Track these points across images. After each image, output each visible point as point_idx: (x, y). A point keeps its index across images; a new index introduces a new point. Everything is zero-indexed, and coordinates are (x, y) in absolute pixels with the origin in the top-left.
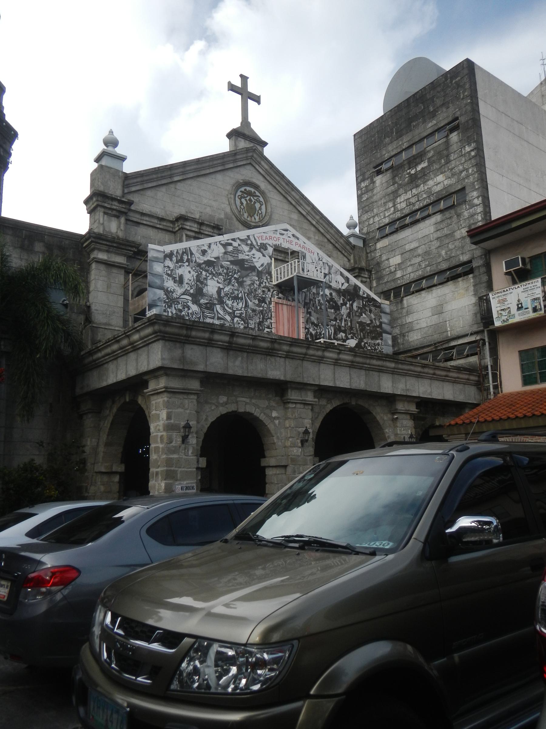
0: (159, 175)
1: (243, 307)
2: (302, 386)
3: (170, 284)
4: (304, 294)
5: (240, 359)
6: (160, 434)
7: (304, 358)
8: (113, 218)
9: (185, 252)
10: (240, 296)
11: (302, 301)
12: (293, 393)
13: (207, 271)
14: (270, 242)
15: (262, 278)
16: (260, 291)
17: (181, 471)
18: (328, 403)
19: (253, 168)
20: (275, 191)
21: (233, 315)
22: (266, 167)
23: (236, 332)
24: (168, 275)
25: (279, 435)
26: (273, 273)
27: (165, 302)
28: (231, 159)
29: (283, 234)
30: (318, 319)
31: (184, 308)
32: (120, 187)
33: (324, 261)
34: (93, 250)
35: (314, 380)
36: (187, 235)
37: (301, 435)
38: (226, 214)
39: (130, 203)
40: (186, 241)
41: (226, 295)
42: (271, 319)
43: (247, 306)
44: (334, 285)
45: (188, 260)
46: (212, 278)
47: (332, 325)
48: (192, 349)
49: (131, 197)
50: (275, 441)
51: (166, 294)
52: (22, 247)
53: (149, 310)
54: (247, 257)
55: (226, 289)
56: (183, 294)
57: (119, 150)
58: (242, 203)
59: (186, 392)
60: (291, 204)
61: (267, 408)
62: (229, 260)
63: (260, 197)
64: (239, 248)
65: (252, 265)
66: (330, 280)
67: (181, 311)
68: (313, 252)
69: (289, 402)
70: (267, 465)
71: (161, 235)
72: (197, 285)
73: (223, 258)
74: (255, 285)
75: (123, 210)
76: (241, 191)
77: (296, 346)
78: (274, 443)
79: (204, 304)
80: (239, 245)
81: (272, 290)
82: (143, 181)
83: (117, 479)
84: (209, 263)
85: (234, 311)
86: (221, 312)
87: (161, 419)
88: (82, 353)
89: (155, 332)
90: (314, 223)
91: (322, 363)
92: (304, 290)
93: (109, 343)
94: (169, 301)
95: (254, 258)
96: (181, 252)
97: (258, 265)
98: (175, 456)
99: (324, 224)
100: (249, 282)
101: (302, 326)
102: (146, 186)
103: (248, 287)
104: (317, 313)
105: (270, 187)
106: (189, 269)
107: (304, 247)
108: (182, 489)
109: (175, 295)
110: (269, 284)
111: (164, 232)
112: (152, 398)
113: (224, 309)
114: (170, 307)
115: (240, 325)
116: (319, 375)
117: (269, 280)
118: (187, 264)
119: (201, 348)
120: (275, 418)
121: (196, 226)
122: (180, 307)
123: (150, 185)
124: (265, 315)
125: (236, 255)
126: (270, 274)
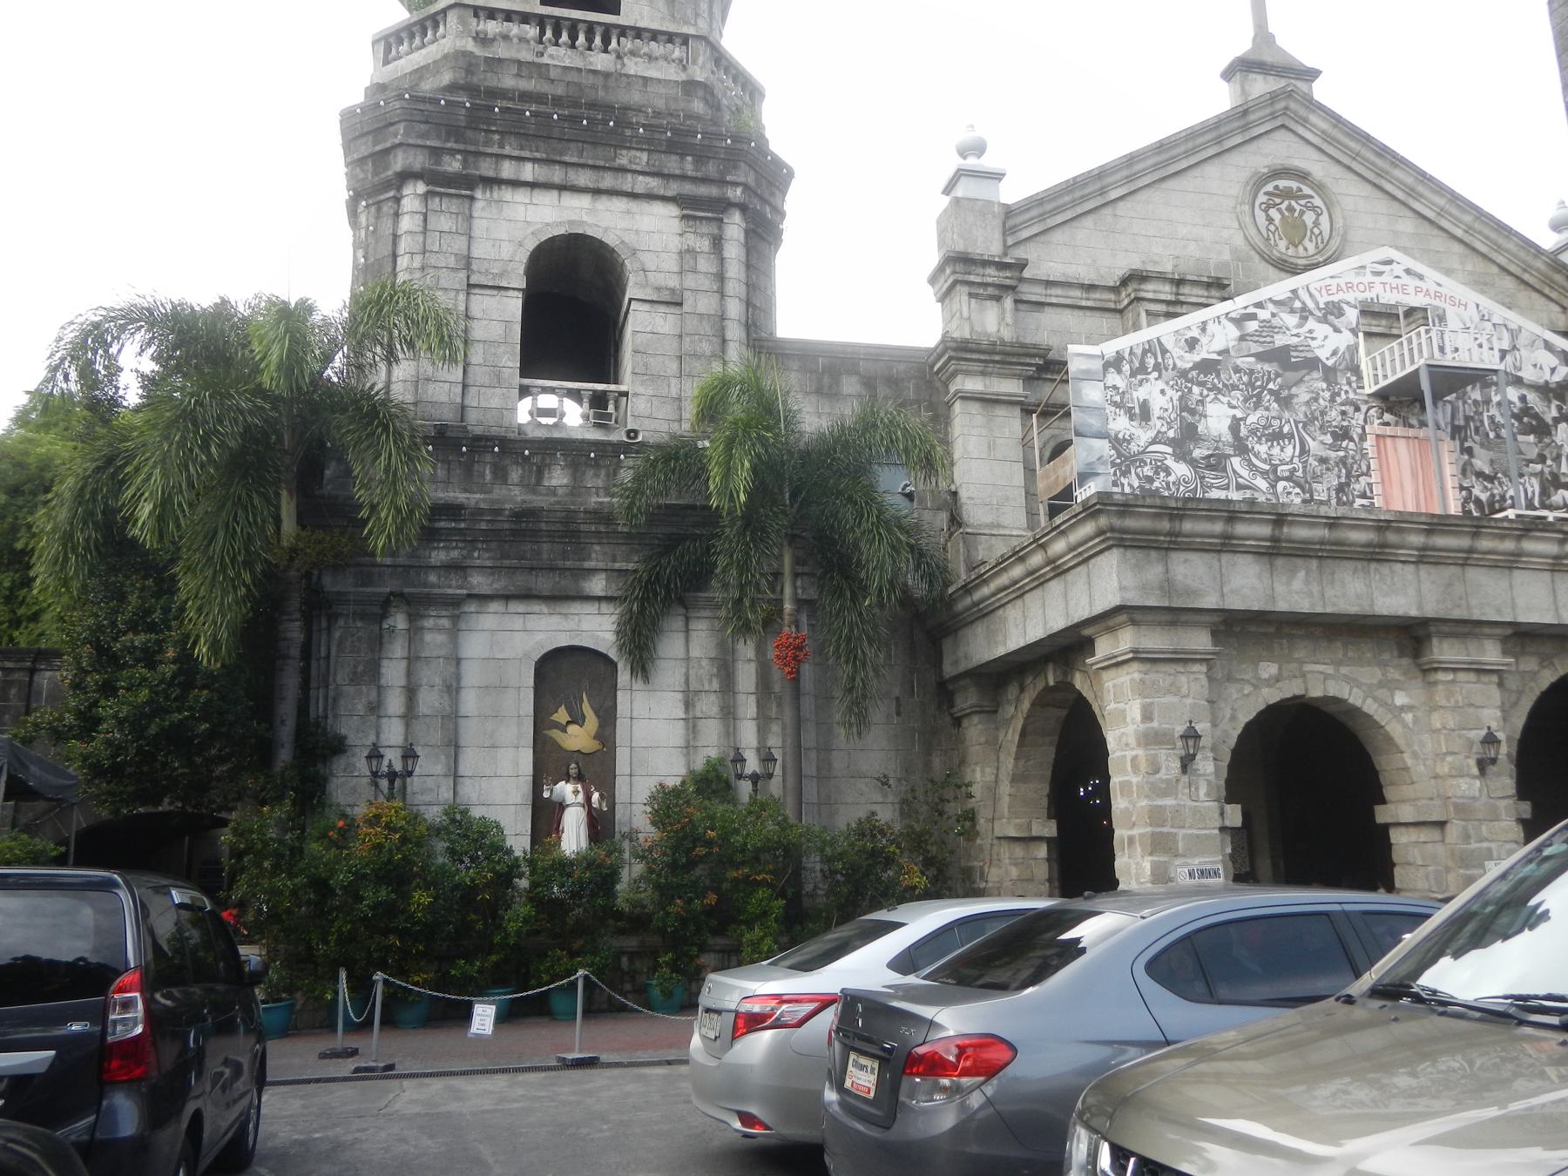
0: (1078, 194)
1: (1297, 453)
2: (1467, 629)
3: (1121, 424)
4: (1449, 408)
5: (1302, 574)
6: (1129, 754)
7: (1467, 559)
8: (988, 303)
9: (1149, 351)
10: (1286, 429)
11: (1446, 424)
13: (1202, 384)
14: (1350, 297)
15: (1337, 384)
16: (1334, 413)
17: (1185, 836)
18: (1544, 667)
19: (1292, 135)
20: (1350, 176)
21: (1273, 476)
22: (1323, 125)
23: (1286, 515)
24: (1115, 404)
25: (1416, 748)
26: (1363, 367)
27: (1113, 464)
28: (1236, 124)
29: (1380, 274)
30: (1492, 462)
31: (1157, 473)
32: (998, 235)
33: (1496, 320)
34: (954, 375)
35: (1499, 611)
36: (1148, 313)
37: (1477, 748)
38: (1234, 251)
39: (1021, 265)
40: (1149, 326)
41: (1253, 432)
42: (1368, 474)
43: (1304, 451)
44: (1528, 374)
45: (1157, 367)
46: (1216, 398)
47: (1534, 475)
48: (1186, 561)
49: (1020, 253)
50: (1409, 762)
51: (1114, 448)
52: (819, 392)
53: (1080, 487)
54: (1295, 340)
55: (1252, 419)
56: (1154, 442)
57: (987, 162)
58: (1270, 220)
59: (1180, 659)
60: (1394, 198)
62: (1252, 351)
63: (1312, 197)
64: (1275, 322)
65: (1309, 355)
66: (1518, 364)
67: (1150, 480)
68: (1463, 302)
69: (1436, 670)
70: (1390, 820)
72: (1182, 418)
73: (1239, 350)
74: (1321, 401)
75: (1008, 282)
76: (1266, 193)
77: (1443, 532)
78: (1406, 769)
79: (1203, 458)
80: (1273, 315)
81: (1364, 408)
82: (1044, 213)
83: (1042, 851)
84: (1206, 366)
85: (1275, 468)
86: (1244, 473)
87: (1128, 720)
88: (950, 591)
89: (1100, 532)
90: (1459, 233)
91: (1517, 568)
92: (1448, 398)
93: (1002, 564)
94: (1122, 462)
95: (1313, 339)
96: (1139, 352)
97: (1323, 354)
98: (1169, 802)
99: (1487, 231)
100: (1305, 397)
101: (1450, 483)
102: (1051, 222)
103: (1304, 408)
104: (1488, 449)
105: (1336, 171)
106: (1161, 385)
107: (1437, 295)
108: (1191, 875)
109: (1134, 448)
110: (1356, 394)
111: (1098, 314)
112: (1105, 675)
113: (1251, 464)
114: (1125, 473)
115: (1292, 497)
116: (1513, 599)
117: (1354, 385)
118: (1155, 374)
119: (1206, 556)
120: (1402, 709)
121: (1167, 288)
122: (1148, 471)
123: (1059, 219)
124: (1351, 470)
125: (1268, 339)
126: (1356, 370)
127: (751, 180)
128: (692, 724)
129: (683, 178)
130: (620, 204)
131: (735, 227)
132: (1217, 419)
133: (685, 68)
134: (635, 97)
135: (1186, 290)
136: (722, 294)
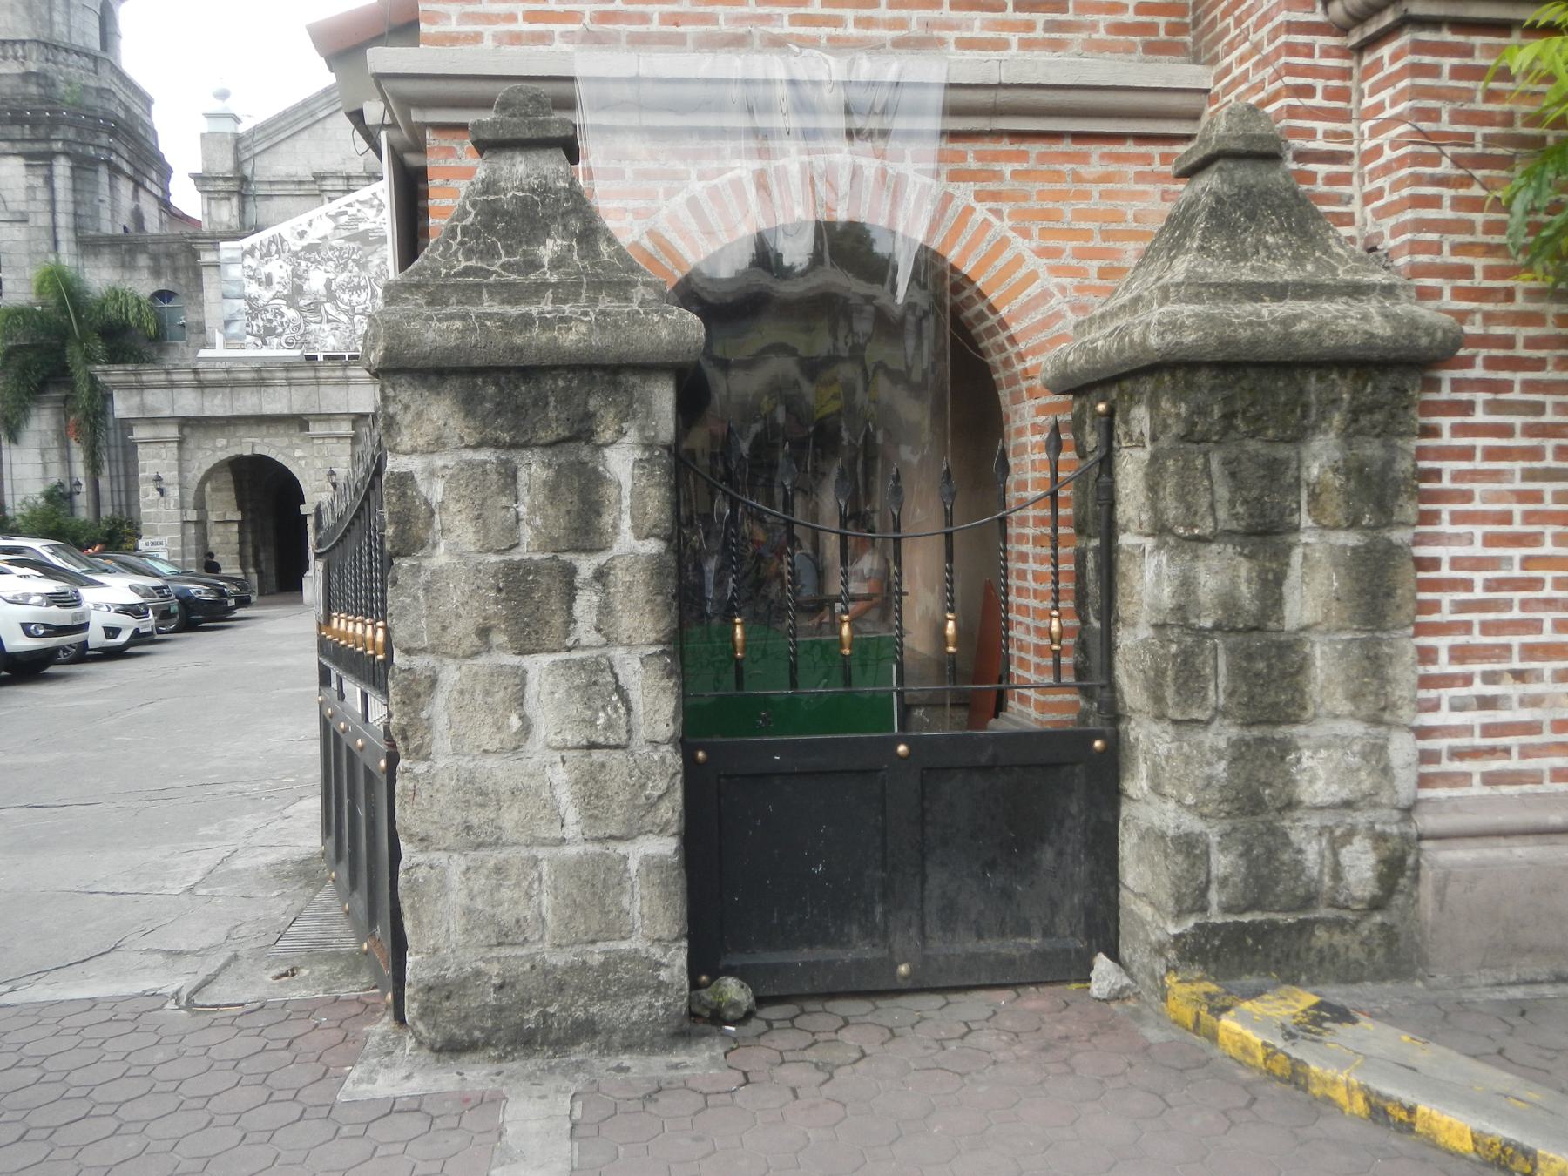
0: (291, 119)
2: (328, 417)
5: (220, 396)
7: (318, 382)
12: (317, 425)
21: (351, 313)
24: (250, 277)
27: (247, 314)
35: (338, 408)
41: (340, 287)
45: (278, 252)
52: (123, 266)
55: (342, 278)
56: (274, 298)
61: (287, 447)
64: (359, 215)
67: (270, 321)
71: (305, 202)
73: (333, 235)
75: (232, 189)
83: (235, 528)
84: (311, 248)
86: (333, 312)
96: (266, 243)
98: (153, 510)
100: (376, 262)
106: (280, 262)
109: (261, 303)
113: (337, 306)
114: (253, 319)
120: (299, 458)
121: (341, 182)
122: (269, 316)
123: (282, 136)
127: (71, 134)
128: (45, 466)
129: (23, 140)
131: (62, 167)
132: (316, 281)
133: (23, 64)
135: (353, 182)
136: (53, 212)
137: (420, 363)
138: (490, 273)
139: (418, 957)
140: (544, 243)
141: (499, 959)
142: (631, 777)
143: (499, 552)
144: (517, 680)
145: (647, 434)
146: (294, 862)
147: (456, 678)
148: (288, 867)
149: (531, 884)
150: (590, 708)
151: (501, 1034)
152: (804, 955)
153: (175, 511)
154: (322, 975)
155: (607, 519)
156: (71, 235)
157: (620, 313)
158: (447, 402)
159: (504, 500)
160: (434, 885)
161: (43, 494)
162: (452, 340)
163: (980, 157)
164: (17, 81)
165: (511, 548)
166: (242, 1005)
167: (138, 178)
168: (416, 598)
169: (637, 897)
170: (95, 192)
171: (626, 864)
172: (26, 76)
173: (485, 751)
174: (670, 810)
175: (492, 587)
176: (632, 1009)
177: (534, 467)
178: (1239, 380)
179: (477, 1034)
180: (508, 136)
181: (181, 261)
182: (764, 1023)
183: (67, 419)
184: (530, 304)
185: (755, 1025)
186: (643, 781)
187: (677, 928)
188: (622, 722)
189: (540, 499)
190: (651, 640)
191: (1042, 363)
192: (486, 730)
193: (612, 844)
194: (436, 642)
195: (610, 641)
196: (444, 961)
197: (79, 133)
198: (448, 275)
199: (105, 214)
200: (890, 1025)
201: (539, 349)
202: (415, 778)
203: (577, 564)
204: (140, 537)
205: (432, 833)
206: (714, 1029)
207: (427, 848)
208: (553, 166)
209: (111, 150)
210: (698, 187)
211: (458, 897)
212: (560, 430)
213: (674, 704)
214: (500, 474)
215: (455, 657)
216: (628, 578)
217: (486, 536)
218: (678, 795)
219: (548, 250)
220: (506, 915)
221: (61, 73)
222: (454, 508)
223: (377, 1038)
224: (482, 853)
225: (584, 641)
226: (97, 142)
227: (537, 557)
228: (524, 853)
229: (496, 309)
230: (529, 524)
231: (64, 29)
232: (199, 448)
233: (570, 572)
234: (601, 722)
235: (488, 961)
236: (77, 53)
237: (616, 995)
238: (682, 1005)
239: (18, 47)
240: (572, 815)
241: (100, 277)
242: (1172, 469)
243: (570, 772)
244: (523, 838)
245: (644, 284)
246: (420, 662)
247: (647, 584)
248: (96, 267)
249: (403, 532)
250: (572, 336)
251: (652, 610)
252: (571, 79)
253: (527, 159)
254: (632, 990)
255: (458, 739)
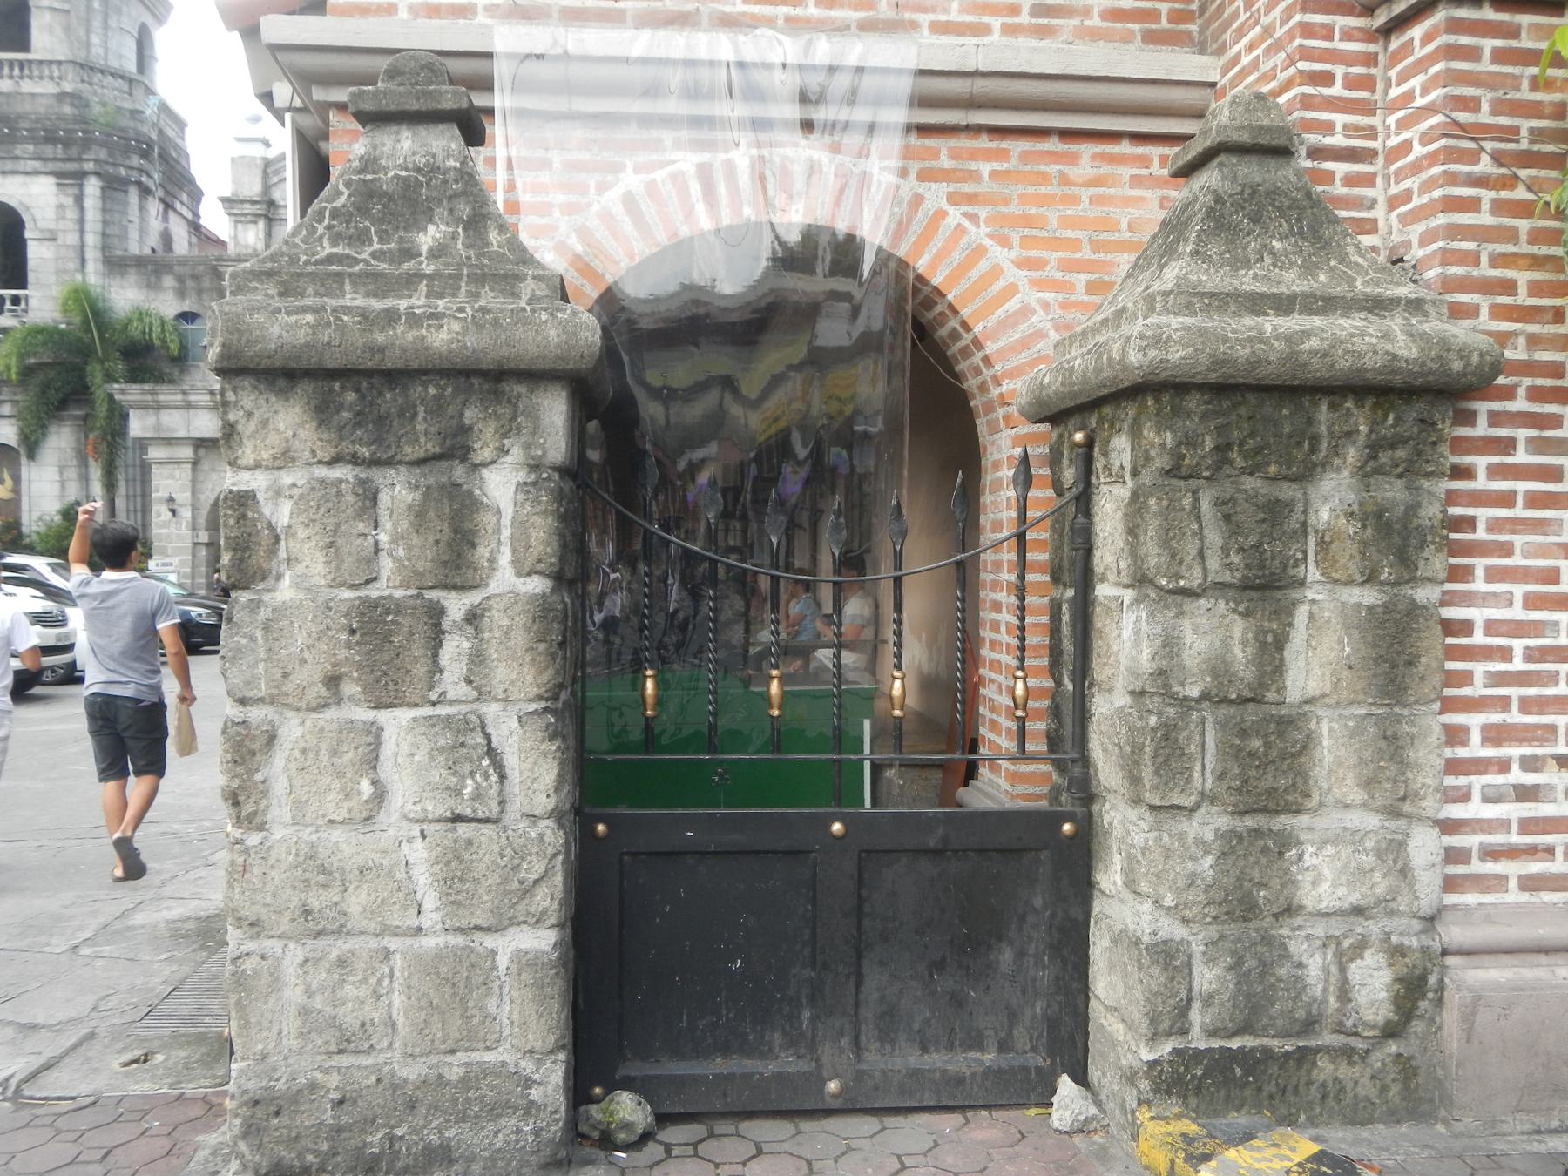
8: (251, 226)
52: (149, 286)
98: (164, 531)
129: (55, 159)
130: (19, 179)
131: (92, 187)
134: (27, 107)
136: (82, 232)
137: (265, 363)
138: (357, 261)
139: (244, 1064)
140: (425, 229)
141: (339, 1069)
142: (502, 857)
143: (353, 587)
144: (370, 739)
145: (533, 453)
146: (198, 919)
147: (299, 734)
148: (191, 925)
149: (379, 982)
150: (455, 774)
151: (339, 1159)
152: (718, 1066)
153: (185, 531)
154: (176, 1063)
155: (483, 552)
156: (99, 254)
157: (502, 311)
158: (298, 409)
159: (361, 526)
160: (265, 979)
161: (59, 512)
162: (302, 337)
163: (954, 154)
164: (52, 101)
165: (368, 582)
166: (73, 1098)
167: (168, 200)
168: (253, 639)
169: (506, 999)
170: (124, 213)
171: (494, 960)
172: (61, 97)
173: (331, 821)
174: (550, 896)
175: (343, 629)
176: (496, 1133)
177: (398, 488)
178: (1235, 406)
179: (310, 1158)
180: (393, 107)
181: (206, 283)
182: (662, 1148)
183: (87, 437)
184: (400, 297)
185: (653, 1150)
186: (516, 861)
187: (552, 1038)
188: (494, 791)
189: (404, 525)
190: (531, 696)
191: (1017, 388)
192: (333, 796)
193: (478, 936)
194: (275, 691)
195: (482, 695)
196: (275, 1069)
197: (111, 154)
198: (307, 263)
199: (134, 234)
200: (809, 1157)
201: (404, 350)
202: (247, 851)
203: (445, 603)
204: (150, 556)
205: (264, 917)
206: (602, 1154)
207: (259, 934)
208: (444, 143)
209: (141, 171)
210: (631, 181)
211: (293, 995)
212: (429, 446)
213: (555, 771)
214: (358, 495)
215: (298, 709)
216: (506, 622)
217: (338, 568)
218: (558, 879)
219: (428, 237)
220: (350, 1017)
221: (95, 93)
222: (302, 533)
223: (207, 1152)
224: (322, 943)
225: (451, 695)
226: (128, 162)
227: (399, 594)
228: (374, 943)
229: (360, 301)
230: (390, 555)
231: (101, 51)
232: (213, 470)
233: (436, 613)
234: (468, 790)
235: (326, 1071)
236: (112, 75)
237: (476, 1116)
238: (556, 1130)
239: (55, 68)
240: (430, 901)
241: (124, 297)
242: (1154, 508)
243: (430, 849)
244: (372, 926)
245: (534, 278)
246: (256, 714)
247: (527, 629)
248: (122, 287)
249: (241, 560)
250: (443, 335)
251: (533, 660)
252: (489, 56)
253: (414, 134)
254: (495, 1111)
255: (299, 806)
